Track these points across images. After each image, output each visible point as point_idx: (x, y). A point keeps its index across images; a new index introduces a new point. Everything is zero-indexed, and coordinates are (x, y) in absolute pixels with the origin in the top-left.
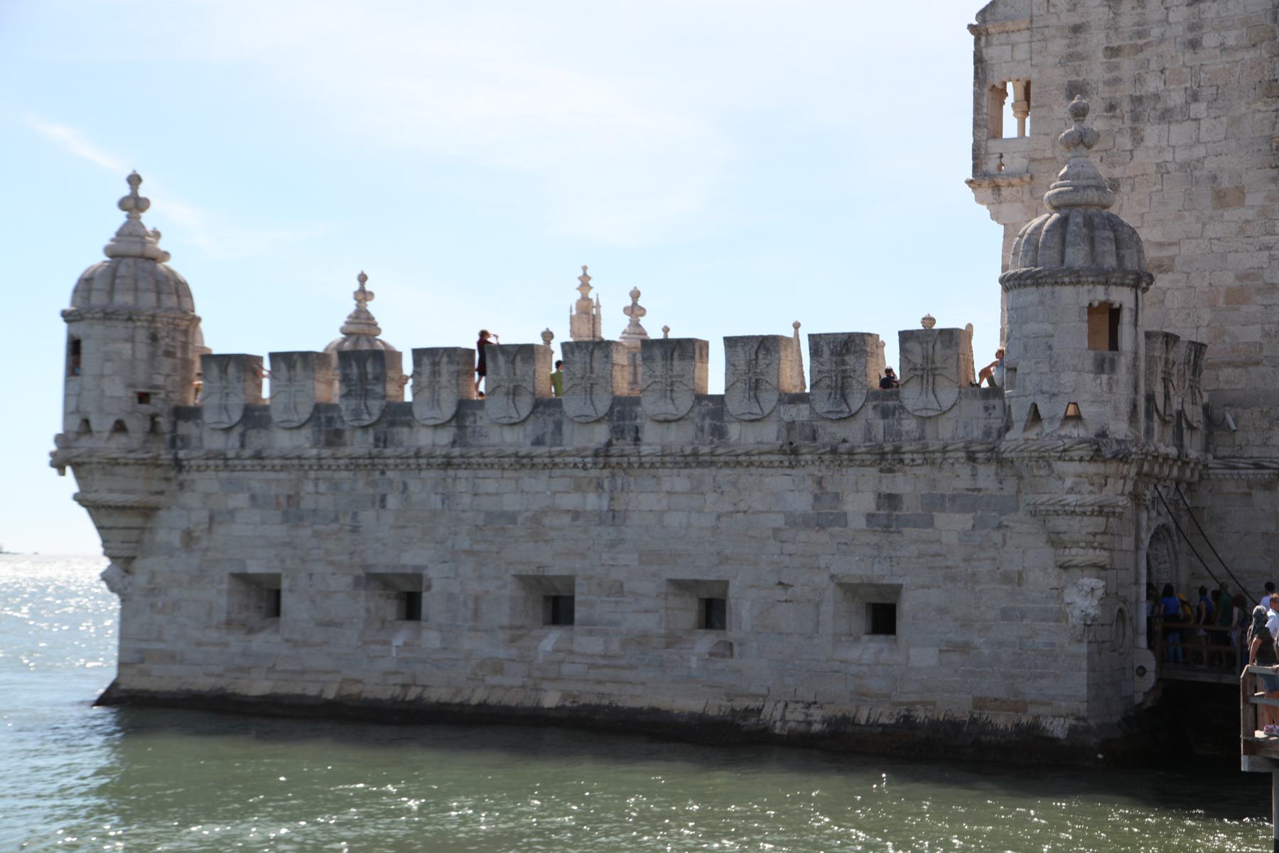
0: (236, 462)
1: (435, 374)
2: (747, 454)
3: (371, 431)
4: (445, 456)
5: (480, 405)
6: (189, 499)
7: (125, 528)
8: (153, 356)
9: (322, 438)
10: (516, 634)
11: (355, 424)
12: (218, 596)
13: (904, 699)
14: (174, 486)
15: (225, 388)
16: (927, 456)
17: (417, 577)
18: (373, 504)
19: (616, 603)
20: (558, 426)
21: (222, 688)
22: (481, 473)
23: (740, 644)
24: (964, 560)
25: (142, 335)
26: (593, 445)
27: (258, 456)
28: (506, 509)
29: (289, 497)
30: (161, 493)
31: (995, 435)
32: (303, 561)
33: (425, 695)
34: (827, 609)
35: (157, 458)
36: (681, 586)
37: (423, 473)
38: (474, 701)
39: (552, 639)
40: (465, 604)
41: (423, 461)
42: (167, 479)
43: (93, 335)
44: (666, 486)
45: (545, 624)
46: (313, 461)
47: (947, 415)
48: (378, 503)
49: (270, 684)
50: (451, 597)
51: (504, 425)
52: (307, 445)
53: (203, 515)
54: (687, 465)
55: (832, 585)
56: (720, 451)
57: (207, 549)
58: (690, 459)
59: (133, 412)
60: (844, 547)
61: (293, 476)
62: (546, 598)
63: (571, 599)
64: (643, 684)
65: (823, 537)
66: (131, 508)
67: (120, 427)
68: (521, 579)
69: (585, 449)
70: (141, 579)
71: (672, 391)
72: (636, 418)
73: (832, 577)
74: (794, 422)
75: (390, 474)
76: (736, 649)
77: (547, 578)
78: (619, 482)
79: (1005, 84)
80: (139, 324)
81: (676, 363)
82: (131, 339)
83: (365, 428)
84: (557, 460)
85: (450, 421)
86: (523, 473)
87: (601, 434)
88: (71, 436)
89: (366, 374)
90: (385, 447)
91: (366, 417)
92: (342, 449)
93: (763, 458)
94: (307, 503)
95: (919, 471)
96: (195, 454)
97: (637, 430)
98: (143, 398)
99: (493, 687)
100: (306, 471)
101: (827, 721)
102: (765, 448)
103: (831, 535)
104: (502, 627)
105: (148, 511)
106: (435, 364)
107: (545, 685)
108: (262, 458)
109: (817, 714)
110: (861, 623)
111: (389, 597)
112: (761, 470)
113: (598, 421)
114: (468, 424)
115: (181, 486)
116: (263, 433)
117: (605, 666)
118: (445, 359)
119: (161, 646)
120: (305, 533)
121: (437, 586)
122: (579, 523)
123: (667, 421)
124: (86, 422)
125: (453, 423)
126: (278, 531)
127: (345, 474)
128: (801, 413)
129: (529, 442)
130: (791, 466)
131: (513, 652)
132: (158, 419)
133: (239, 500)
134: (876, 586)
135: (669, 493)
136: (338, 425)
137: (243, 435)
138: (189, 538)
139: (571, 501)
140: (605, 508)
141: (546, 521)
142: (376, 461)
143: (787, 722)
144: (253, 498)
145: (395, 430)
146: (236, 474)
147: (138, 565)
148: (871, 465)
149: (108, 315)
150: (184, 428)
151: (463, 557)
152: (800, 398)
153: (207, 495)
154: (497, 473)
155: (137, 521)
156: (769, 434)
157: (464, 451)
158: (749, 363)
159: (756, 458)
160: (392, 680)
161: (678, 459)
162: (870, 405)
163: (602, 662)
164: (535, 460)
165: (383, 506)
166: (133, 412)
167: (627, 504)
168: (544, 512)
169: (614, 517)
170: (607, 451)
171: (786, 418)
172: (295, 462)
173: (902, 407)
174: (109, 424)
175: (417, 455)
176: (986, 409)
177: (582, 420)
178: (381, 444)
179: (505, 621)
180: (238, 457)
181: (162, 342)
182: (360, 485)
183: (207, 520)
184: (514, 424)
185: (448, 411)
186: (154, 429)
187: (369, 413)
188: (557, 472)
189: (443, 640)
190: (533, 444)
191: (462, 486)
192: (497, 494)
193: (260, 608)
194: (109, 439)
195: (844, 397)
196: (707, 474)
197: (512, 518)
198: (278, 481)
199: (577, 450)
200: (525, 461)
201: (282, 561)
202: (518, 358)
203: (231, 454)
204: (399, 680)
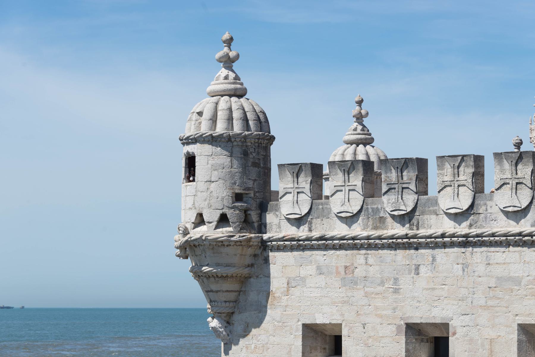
7: (227, 291)
9: (370, 223)
17: (446, 326)
22: (492, 249)
25: (237, 151)
29: (346, 267)
48: (413, 271)
51: (509, 212)
67: (223, 220)
80: (235, 143)
92: (385, 232)
94: (359, 272)
98: (238, 197)
108: (326, 240)
116: (325, 221)
120: (359, 294)
121: (460, 332)
124: (200, 215)
132: (249, 212)
136: (382, 214)
144: (318, 268)
145: (426, 217)
151: (480, 311)
153: (285, 267)
157: (479, 231)
165: (418, 274)
166: (232, 208)
174: (216, 216)
178: (415, 228)
181: (251, 156)
193: (325, 349)
194: (217, 227)
197: (517, 281)
198: (338, 256)
201: (342, 315)
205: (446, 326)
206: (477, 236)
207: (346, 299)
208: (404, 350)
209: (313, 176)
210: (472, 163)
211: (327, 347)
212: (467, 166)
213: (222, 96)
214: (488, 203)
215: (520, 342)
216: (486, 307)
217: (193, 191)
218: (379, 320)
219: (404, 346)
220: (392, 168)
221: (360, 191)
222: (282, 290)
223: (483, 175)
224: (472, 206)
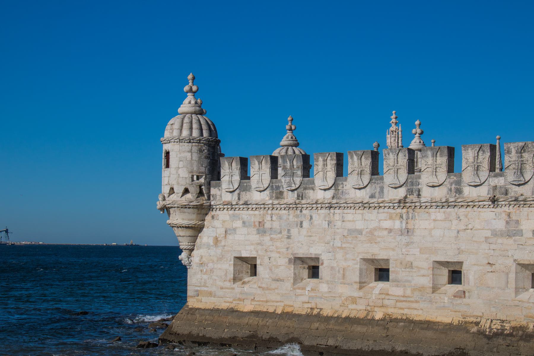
0: (236, 206)
3: (296, 192)
6: (216, 223)
7: (189, 236)
9: (274, 195)
10: (362, 285)
11: (289, 188)
12: (228, 267)
15: (231, 173)
17: (317, 259)
19: (409, 271)
20: (382, 189)
21: (232, 308)
22: (346, 211)
23: (469, 292)
25: (195, 149)
27: (246, 203)
28: (357, 228)
29: (260, 222)
33: (321, 313)
34: (512, 276)
35: (202, 205)
37: (319, 211)
40: (339, 271)
41: (319, 205)
44: (433, 217)
45: (375, 281)
46: (270, 206)
48: (299, 225)
49: (253, 306)
50: (332, 268)
51: (356, 189)
52: (267, 198)
53: (223, 230)
55: (515, 264)
56: (459, 200)
57: (224, 246)
58: (444, 204)
59: (192, 184)
60: (521, 246)
61: (262, 212)
63: (387, 270)
64: (422, 310)
65: (511, 241)
67: (186, 191)
68: (365, 260)
69: (394, 200)
72: (419, 184)
73: (515, 260)
74: (496, 186)
75: (304, 212)
76: (467, 294)
77: (377, 260)
78: (410, 215)
80: (194, 144)
82: (191, 151)
83: (293, 191)
84: (381, 205)
85: (331, 187)
86: (366, 210)
87: (402, 193)
90: (302, 199)
91: (293, 185)
93: (480, 203)
94: (268, 225)
96: (218, 203)
97: (419, 191)
99: (352, 310)
102: (482, 199)
103: (515, 241)
104: (356, 282)
106: (324, 160)
107: (376, 309)
109: (507, 326)
111: (304, 268)
114: (340, 188)
116: (248, 193)
117: (404, 301)
119: (206, 289)
120: (267, 238)
121: (326, 263)
122: (391, 234)
123: (433, 186)
124: (172, 189)
125: (333, 188)
126: (255, 237)
129: (368, 197)
131: (361, 294)
132: (203, 187)
136: (281, 190)
137: (239, 194)
138: (216, 240)
139: (387, 224)
140: (404, 227)
141: (376, 233)
142: (298, 206)
143: (492, 329)
144: (244, 223)
145: (307, 191)
146: (236, 212)
147: (194, 253)
153: (224, 222)
154: (352, 211)
156: (484, 192)
157: (338, 201)
159: (477, 203)
160: (306, 306)
161: (439, 204)
163: (402, 299)
164: (371, 205)
165: (302, 227)
166: (192, 184)
167: (414, 225)
168: (375, 229)
169: (408, 231)
170: (405, 200)
172: (262, 206)
174: (182, 190)
175: (316, 203)
178: (300, 198)
182: (291, 217)
183: (224, 233)
188: (381, 210)
189: (329, 288)
190: (370, 197)
191: (337, 217)
192: (353, 221)
194: (182, 196)
197: (360, 232)
198: (255, 215)
199: (391, 200)
200: (365, 205)
201: (257, 251)
202: (363, 157)
203: (234, 203)
204: (310, 306)
205: (317, 259)
207: (259, 242)
208: (293, 274)
209: (241, 165)
210: (335, 158)
211: (249, 271)
212: (332, 160)
214: (344, 183)
215: (361, 270)
216: (341, 248)
217: (168, 173)
218: (278, 255)
219: (293, 271)
220: (288, 160)
222: (222, 236)
223: (342, 165)
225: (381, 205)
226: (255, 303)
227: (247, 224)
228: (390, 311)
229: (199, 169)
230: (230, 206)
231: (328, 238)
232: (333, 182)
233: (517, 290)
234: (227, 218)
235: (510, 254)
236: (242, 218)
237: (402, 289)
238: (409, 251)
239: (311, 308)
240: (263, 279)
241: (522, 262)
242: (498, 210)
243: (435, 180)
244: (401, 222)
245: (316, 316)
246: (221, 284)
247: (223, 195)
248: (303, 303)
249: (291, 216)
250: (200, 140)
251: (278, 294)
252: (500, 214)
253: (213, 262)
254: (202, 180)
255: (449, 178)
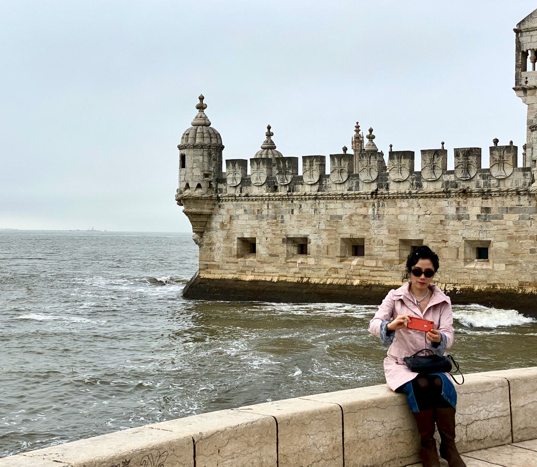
1: (311, 165)
2: (430, 193)
3: (288, 187)
4: (315, 195)
5: (328, 176)
6: (222, 211)
8: (209, 160)
11: (282, 184)
12: (235, 245)
13: (492, 282)
14: (217, 207)
16: (502, 193)
18: (289, 213)
20: (358, 183)
22: (329, 201)
24: (515, 231)
25: (206, 153)
26: (371, 191)
27: (247, 195)
28: (338, 214)
29: (258, 210)
30: (213, 209)
31: (527, 185)
32: (264, 233)
34: (462, 250)
35: (211, 197)
36: (404, 242)
38: (328, 283)
39: (356, 261)
42: (214, 204)
43: (189, 154)
45: (353, 255)
47: (510, 178)
50: (318, 246)
52: (264, 192)
54: (407, 198)
58: (408, 195)
62: (353, 246)
66: (203, 215)
67: (199, 186)
70: (206, 240)
71: (401, 170)
75: (295, 202)
78: (381, 204)
79: (527, 51)
81: (402, 160)
82: (203, 155)
84: (357, 196)
87: (374, 187)
88: (182, 189)
89: (286, 166)
90: (293, 192)
94: (265, 213)
95: (498, 199)
98: (206, 176)
99: (334, 278)
100: (264, 201)
101: (461, 289)
102: (438, 191)
104: (337, 257)
105: (210, 216)
106: (310, 162)
107: (354, 277)
109: (458, 288)
110: (473, 255)
111: (295, 246)
112: (436, 199)
113: (373, 182)
115: (220, 207)
116: (248, 187)
117: (376, 271)
118: (315, 160)
119: (214, 263)
120: (264, 223)
121: (313, 242)
122: (366, 219)
123: (399, 182)
124: (187, 185)
127: (277, 202)
128: (452, 178)
129: (346, 190)
130: (447, 197)
133: (241, 211)
134: (480, 241)
135: (400, 208)
136: (276, 184)
137: (241, 189)
138: (223, 225)
139: (363, 211)
140: (376, 213)
141: (353, 218)
144: (245, 211)
146: (239, 202)
148: (479, 197)
149: (195, 147)
150: (220, 186)
152: (452, 172)
155: (205, 219)
157: (323, 193)
158: (431, 159)
160: (297, 275)
162: (478, 175)
163: (375, 269)
167: (384, 212)
168: (352, 215)
171: (445, 180)
172: (260, 198)
173: (491, 175)
175: (305, 195)
176: (524, 175)
177: (367, 181)
179: (339, 255)
180: (240, 196)
184: (341, 183)
185: (316, 179)
186: (210, 187)
187: (287, 180)
188: (357, 200)
191: (322, 206)
195: (468, 172)
196: (415, 201)
197: (340, 217)
203: (237, 195)
206: (322, 195)
213: (199, 125)
218: (274, 236)
221: (265, 173)
223: (325, 165)
224: (319, 181)
225: (357, 196)
226: (255, 274)
227: (248, 212)
228: (365, 278)
229: (209, 168)
230: (235, 198)
231: (315, 222)
232: (318, 179)
233: (466, 261)
234: (232, 207)
235: (460, 233)
236: (244, 207)
237: (375, 261)
238: (380, 232)
239: (301, 277)
240: (261, 254)
241: (469, 239)
242: (449, 199)
243: (401, 177)
244: (374, 210)
245: (305, 283)
246: (227, 259)
247: (228, 189)
248: (295, 273)
249: (284, 206)
250: (210, 146)
251: (274, 266)
252: (452, 202)
253: (220, 242)
254: (211, 178)
255: (411, 175)
